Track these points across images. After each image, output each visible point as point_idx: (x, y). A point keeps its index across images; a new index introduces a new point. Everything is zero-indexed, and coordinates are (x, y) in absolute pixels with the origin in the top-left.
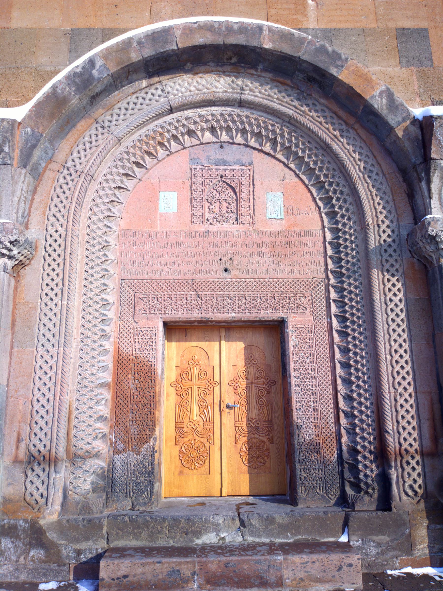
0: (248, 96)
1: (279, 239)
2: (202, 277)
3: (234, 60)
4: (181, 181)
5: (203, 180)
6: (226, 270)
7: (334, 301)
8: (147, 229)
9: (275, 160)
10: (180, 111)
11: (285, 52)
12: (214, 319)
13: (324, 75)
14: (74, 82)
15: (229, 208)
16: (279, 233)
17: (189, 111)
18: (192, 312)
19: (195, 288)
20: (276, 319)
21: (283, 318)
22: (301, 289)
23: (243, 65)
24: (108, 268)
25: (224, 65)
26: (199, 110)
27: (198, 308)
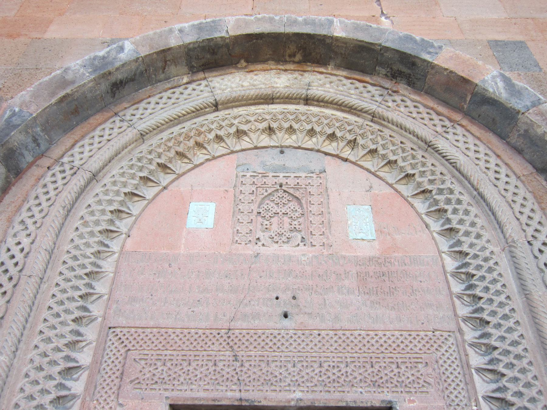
0: (316, 91)
2: (245, 325)
3: (298, 57)
4: (222, 189)
5: (254, 189)
6: (286, 316)
7: (479, 370)
8: (164, 252)
9: (356, 167)
10: (228, 108)
11: (362, 39)
12: (264, 403)
13: (414, 64)
14: (93, 64)
15: (291, 225)
16: (370, 259)
17: (240, 109)
21: (390, 402)
22: (416, 350)
23: (309, 64)
24: (90, 307)
25: (285, 62)
26: (253, 108)
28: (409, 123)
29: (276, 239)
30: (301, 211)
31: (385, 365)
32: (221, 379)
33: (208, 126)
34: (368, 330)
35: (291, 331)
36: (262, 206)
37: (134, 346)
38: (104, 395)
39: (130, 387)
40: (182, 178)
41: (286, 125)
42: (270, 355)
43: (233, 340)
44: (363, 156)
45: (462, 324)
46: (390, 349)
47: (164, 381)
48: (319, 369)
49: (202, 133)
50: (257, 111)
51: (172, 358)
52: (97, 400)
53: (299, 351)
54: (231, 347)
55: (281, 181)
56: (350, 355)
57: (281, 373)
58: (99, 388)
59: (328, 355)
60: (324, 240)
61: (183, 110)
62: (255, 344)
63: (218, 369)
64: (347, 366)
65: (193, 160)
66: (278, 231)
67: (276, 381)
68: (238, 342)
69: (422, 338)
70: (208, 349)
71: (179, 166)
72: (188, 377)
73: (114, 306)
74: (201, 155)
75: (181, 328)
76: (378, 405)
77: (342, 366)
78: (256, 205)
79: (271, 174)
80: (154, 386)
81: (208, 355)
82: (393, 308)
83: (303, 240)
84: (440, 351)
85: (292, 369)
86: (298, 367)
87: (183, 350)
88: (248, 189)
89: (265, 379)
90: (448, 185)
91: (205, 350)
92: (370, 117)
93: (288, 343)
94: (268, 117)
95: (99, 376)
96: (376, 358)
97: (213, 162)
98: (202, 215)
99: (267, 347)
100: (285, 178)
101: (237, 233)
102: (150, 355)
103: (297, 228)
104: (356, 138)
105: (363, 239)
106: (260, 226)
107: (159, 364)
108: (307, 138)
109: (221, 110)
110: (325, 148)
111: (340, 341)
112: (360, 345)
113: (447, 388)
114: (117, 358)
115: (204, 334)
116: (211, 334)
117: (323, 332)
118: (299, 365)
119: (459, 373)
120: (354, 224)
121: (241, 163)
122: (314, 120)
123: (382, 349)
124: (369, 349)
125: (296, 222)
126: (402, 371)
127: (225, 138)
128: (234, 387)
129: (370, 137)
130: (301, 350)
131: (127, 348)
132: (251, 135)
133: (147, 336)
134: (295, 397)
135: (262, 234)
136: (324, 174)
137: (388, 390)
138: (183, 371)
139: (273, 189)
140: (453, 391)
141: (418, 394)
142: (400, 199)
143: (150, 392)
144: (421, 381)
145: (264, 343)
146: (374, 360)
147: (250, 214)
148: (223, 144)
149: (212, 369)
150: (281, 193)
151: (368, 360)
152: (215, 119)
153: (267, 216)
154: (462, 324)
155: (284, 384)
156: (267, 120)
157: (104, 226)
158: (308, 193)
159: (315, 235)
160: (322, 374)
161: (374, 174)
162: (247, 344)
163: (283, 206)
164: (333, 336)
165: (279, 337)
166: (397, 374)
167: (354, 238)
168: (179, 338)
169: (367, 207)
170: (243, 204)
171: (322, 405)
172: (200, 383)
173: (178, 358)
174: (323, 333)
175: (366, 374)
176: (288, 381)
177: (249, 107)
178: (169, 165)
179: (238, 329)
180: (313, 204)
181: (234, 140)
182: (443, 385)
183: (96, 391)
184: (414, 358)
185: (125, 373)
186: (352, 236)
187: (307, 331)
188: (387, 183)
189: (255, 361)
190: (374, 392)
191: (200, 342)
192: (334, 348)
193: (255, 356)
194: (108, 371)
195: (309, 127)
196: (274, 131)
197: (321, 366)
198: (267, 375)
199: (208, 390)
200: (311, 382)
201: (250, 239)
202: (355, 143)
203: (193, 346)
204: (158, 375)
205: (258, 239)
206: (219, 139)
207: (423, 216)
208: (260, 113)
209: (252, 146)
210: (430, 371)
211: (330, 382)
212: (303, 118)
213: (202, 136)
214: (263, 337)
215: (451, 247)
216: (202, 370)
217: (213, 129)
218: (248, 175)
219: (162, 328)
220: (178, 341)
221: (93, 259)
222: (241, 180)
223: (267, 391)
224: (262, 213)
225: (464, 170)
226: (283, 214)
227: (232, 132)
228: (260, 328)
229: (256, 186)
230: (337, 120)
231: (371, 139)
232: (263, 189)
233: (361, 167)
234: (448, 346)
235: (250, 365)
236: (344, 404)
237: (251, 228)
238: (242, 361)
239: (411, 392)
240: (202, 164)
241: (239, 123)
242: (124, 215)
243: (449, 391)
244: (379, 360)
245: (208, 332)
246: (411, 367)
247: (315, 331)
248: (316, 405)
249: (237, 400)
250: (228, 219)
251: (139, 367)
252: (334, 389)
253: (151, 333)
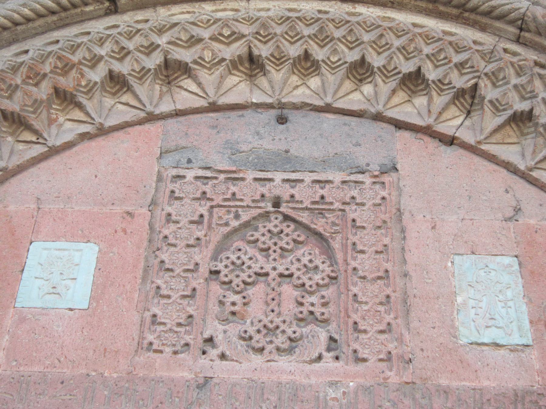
4: (118, 209)
9: (477, 160)
15: (302, 304)
17: (176, 9)
29: (259, 340)
30: (328, 270)
33: (89, 49)
36: (223, 256)
41: (294, 51)
44: (496, 131)
49: (73, 66)
50: (220, 15)
55: (277, 192)
60: (391, 346)
61: (24, 5)
65: (45, 135)
66: (266, 321)
74: (69, 125)
78: (208, 252)
79: (250, 175)
83: (333, 345)
88: (186, 210)
92: (512, 29)
94: (245, 29)
97: (101, 141)
98: (61, 275)
100: (287, 185)
101: (153, 323)
103: (318, 315)
104: (476, 86)
105: (497, 345)
106: (217, 309)
108: (348, 85)
109: (124, 12)
110: (396, 110)
120: (472, 303)
121: (172, 145)
122: (366, 37)
125: (313, 299)
127: (132, 81)
129: (515, 81)
132: (203, 74)
135: (221, 327)
136: (394, 175)
139: (255, 212)
147: (189, 275)
148: (127, 98)
150: (276, 222)
152: (108, 32)
153: (236, 281)
156: (244, 36)
158: (350, 224)
159: (365, 331)
161: (525, 176)
163: (282, 257)
167: (473, 339)
169: (507, 260)
170: (172, 249)
177: (197, 5)
180: (362, 252)
181: (157, 87)
186: (467, 334)
195: (353, 56)
196: (262, 67)
201: (188, 338)
202: (473, 97)
205: (210, 340)
206: (117, 82)
208: (227, 20)
209: (202, 103)
212: (338, 34)
213: (74, 73)
217: (101, 58)
218: (190, 175)
222: (171, 187)
224: (224, 271)
226: (281, 275)
227: (152, 67)
229: (209, 204)
230: (428, 38)
231: (515, 86)
232: (229, 212)
237: (191, 310)
240: (68, 146)
241: (169, 43)
250: (128, 287)
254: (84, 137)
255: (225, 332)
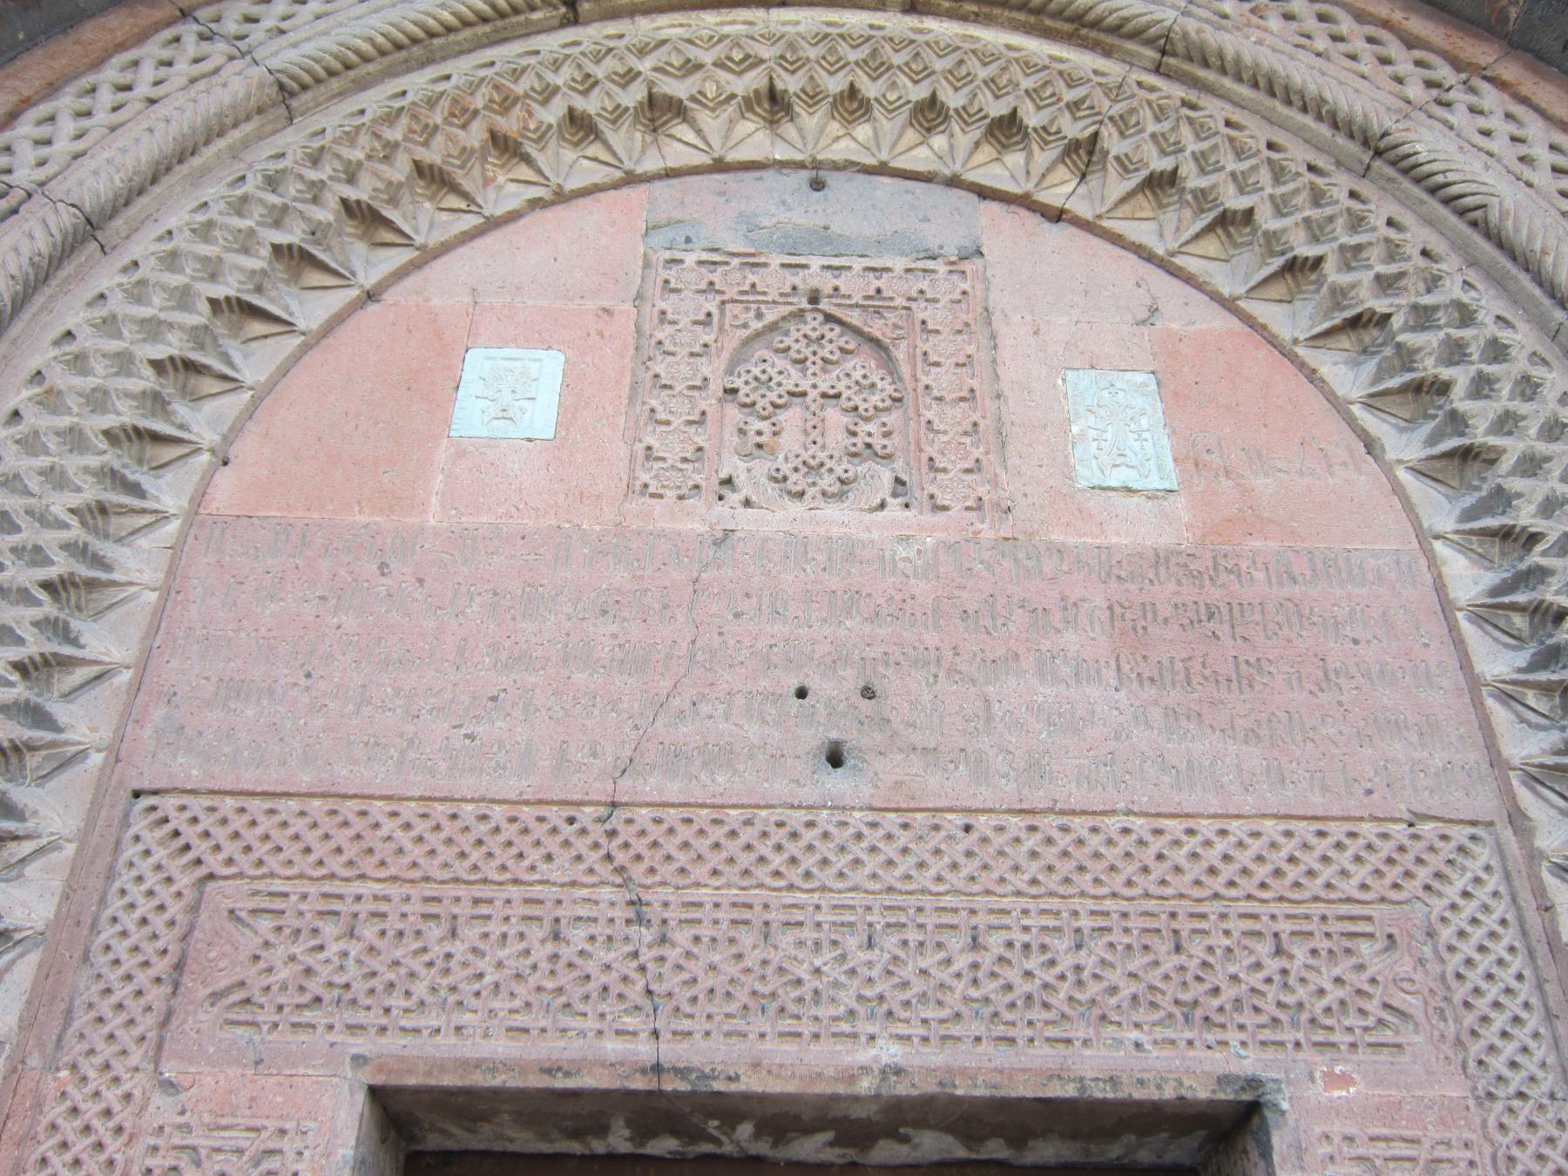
1: (1165, 593)
2: (674, 790)
4: (590, 304)
8: (364, 519)
9: (1095, 241)
12: (752, 1083)
15: (854, 434)
16: (1160, 559)
17: (663, 20)
18: (591, 1024)
19: (621, 857)
20: (1202, 1092)
21: (1253, 1083)
22: (1349, 887)
24: (60, 711)
27: (635, 993)
28: (1301, 72)
29: (797, 481)
30: (890, 389)
31: (1227, 942)
32: (580, 991)
33: (539, 76)
34: (1159, 815)
35: (857, 814)
36: (742, 368)
37: (230, 861)
38: (100, 1046)
39: (206, 1016)
40: (437, 265)
41: (835, 85)
42: (774, 903)
43: (626, 845)
44: (1123, 200)
45: (1525, 796)
46: (1248, 885)
47: (349, 996)
48: (970, 957)
49: (517, 99)
50: (727, 29)
51: (383, 907)
52: (74, 1067)
53: (890, 889)
54: (620, 870)
55: (815, 283)
56: (1090, 904)
57: (817, 971)
58: (82, 1020)
59: (1006, 903)
60: (982, 491)
61: (443, 6)
62: (715, 860)
63: (567, 953)
64: (1079, 947)
65: (479, 200)
66: (805, 456)
67: (800, 1000)
68: (646, 853)
69: (1369, 847)
70: (527, 877)
71: (427, 220)
72: (445, 982)
73: (158, 713)
74: (512, 187)
75: (421, 798)
76: (1203, 1094)
77: (1061, 944)
78: (721, 363)
79: (776, 260)
80: (308, 1016)
81: (527, 901)
82: (1252, 735)
83: (900, 489)
84: (1440, 894)
85: (865, 956)
86: (887, 946)
87: (427, 879)
88: (688, 307)
89: (754, 993)
90: (1452, 290)
91: (516, 881)
92: (1150, 53)
93: (845, 860)
94: (765, 52)
95: (86, 973)
96: (1192, 915)
97: (560, 211)
98: (511, 394)
99: (762, 873)
100: (829, 274)
101: (648, 458)
102: (294, 898)
103: (878, 448)
104: (1096, 134)
105: (1129, 490)
106: (736, 439)
107: (329, 929)
108: (911, 136)
109: (588, 22)
110: (980, 171)
111: (1050, 854)
112: (1130, 869)
113: (1474, 1033)
114: (162, 908)
115: (513, 820)
116: (541, 819)
117: (983, 818)
118: (891, 942)
119: (1520, 977)
120: (1092, 434)
121: (662, 218)
122: (939, 65)
123: (1218, 884)
124: (1163, 882)
126: (1295, 967)
127: (602, 125)
128: (630, 1022)
129: (1152, 127)
130: (898, 885)
131: (202, 871)
132: (704, 117)
133: (285, 824)
134: (876, 1059)
135: (742, 465)
136: (978, 261)
137: (1243, 1036)
138: (426, 958)
139: (785, 310)
140: (1499, 1043)
141: (1362, 1055)
142: (1264, 352)
143: (290, 1037)
144: (1373, 1006)
145: (753, 856)
146: (1185, 925)
147: (696, 393)
148: (595, 149)
149: (541, 953)
150: (815, 324)
151: (1162, 922)
152: (567, 51)
153: (761, 403)
154: (1525, 796)
155: (833, 1012)
156: (762, 61)
157: (126, 415)
158: (918, 326)
159: (945, 470)
160: (980, 974)
161: (1164, 264)
162: (682, 858)
163: (824, 370)
164: (1023, 835)
165: (809, 836)
166: (1277, 978)
167: (1096, 482)
168: (413, 834)
169: (1140, 378)
170: (670, 358)
171: (981, 1092)
172: (496, 1005)
173: (406, 908)
174: (982, 822)
175: (1154, 977)
176: (847, 999)
177: (694, 14)
178: (389, 213)
179: (648, 805)
180: (937, 364)
181: (639, 135)
182: (1458, 1020)
183: (70, 1031)
184: (1340, 918)
185: (191, 965)
186: (1087, 475)
187: (919, 816)
188: (1215, 297)
189: (716, 922)
190: (1190, 1043)
191: (497, 851)
192: (1026, 877)
193: (717, 905)
194: (124, 956)
195: (920, 93)
196: (788, 109)
197: (975, 944)
198: (763, 977)
199: (526, 1031)
200: (940, 1003)
201: (697, 478)
202: (1091, 153)
203: (467, 863)
204: (325, 973)
205: (728, 482)
206: (580, 126)
207: (1356, 410)
208: (739, 36)
210: (1405, 967)
211: (1012, 1005)
212: (898, 59)
213: (517, 111)
214: (747, 835)
215: (1469, 515)
216: (502, 954)
217: (557, 89)
218: (690, 259)
219: (345, 796)
220: (408, 845)
221: (76, 532)
222: (664, 274)
223: (762, 1036)
224: (744, 390)
225: (1517, 230)
226: (824, 395)
227: (632, 105)
228: (734, 801)
229: (719, 298)
230: (1028, 66)
231: (1153, 136)
232: (748, 309)
233: (1116, 239)
234: (1469, 875)
235: (697, 939)
236: (1070, 1091)
237: (700, 441)
238: (664, 922)
239: (1333, 1045)
240: (513, 217)
241: (656, 69)
242: (208, 385)
243: (1483, 1043)
244: (1203, 925)
245: (528, 814)
246: (1330, 951)
247: (949, 816)
248: (959, 1092)
249: (644, 1071)
250: (610, 409)
251: (249, 942)
252: (1029, 1032)
253: (302, 814)
254: (536, 204)
255: (749, 470)
